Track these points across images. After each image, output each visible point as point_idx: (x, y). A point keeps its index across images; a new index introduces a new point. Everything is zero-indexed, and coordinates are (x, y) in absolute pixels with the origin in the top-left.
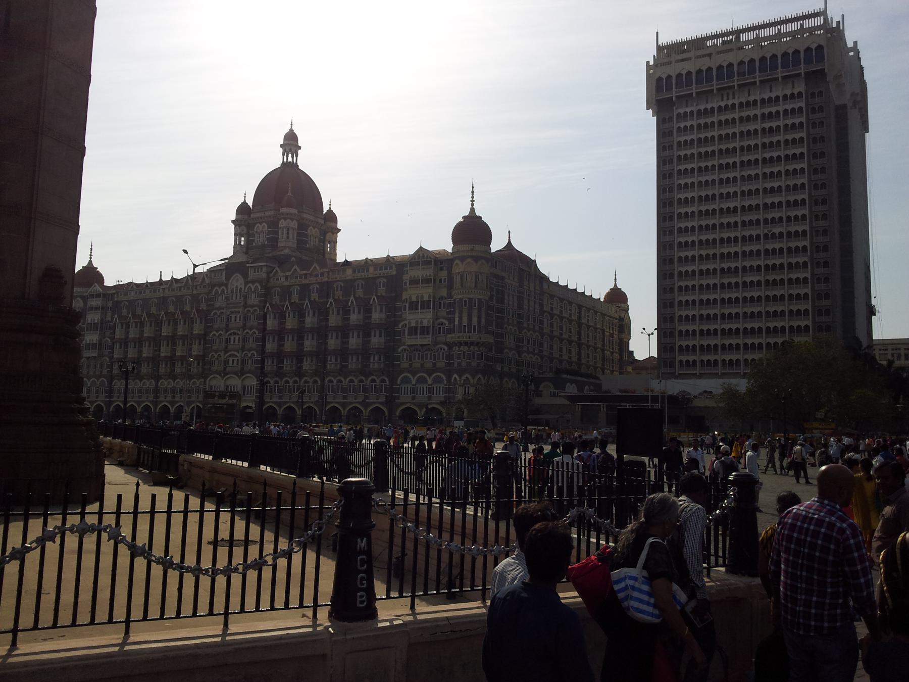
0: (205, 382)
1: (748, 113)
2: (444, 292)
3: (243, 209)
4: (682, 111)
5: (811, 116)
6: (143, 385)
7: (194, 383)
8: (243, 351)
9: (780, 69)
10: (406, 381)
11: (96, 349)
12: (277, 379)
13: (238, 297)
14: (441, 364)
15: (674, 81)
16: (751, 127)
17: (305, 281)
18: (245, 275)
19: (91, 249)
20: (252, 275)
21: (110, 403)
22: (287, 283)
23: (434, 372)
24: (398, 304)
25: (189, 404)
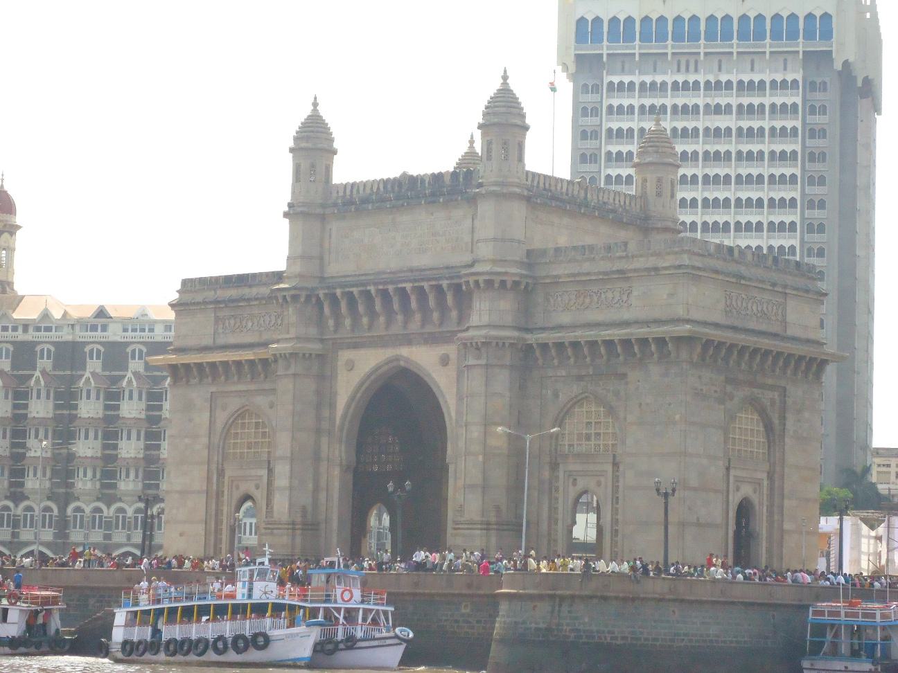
1: (718, 100)
4: (616, 79)
5: (809, 119)
16: (722, 122)
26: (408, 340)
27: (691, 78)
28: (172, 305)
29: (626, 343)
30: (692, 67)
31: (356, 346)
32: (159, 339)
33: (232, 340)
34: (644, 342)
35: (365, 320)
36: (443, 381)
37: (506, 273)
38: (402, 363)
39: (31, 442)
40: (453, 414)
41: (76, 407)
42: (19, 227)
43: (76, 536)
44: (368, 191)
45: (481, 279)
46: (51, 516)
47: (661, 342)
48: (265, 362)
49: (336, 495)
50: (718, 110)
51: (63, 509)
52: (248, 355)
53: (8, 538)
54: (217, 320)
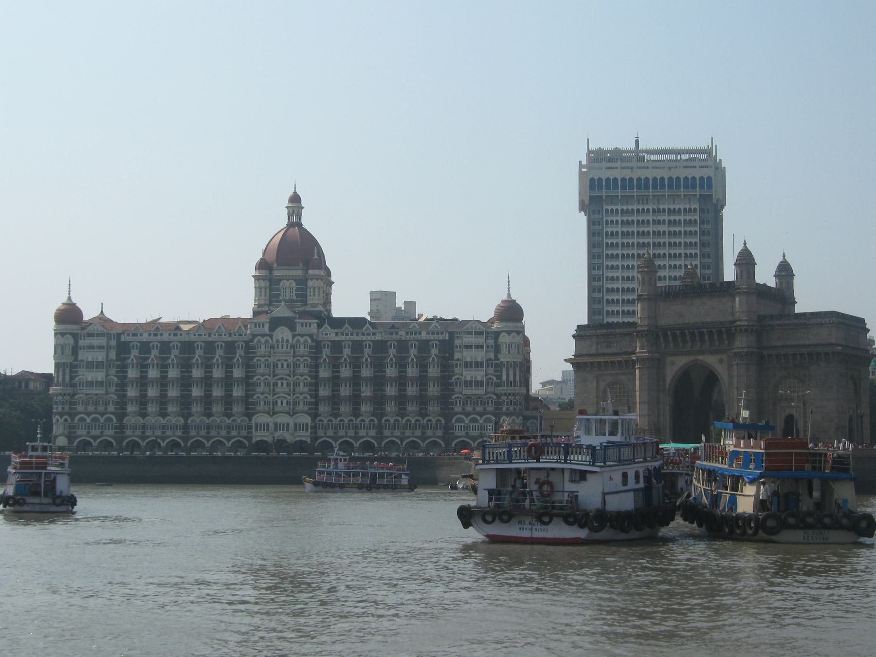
0: (250, 420)
2: (492, 356)
3: (262, 265)
4: (609, 208)
6: (167, 421)
7: (234, 420)
8: (294, 394)
9: (682, 189)
10: (460, 420)
11: (103, 386)
12: (332, 418)
13: (285, 347)
14: (490, 408)
15: (604, 184)
16: (661, 228)
17: (355, 337)
18: (292, 328)
19: (70, 285)
20: (299, 329)
21: (123, 439)
22: (337, 339)
23: (484, 414)
24: (450, 362)
25: (228, 439)
26: (702, 353)
27: (646, 207)
28: (574, 336)
29: (810, 355)
30: (645, 202)
31: (675, 355)
32: (425, 338)
33: (606, 351)
34: (818, 354)
35: (681, 344)
36: (721, 370)
37: (753, 325)
38: (699, 362)
39: (363, 389)
40: (727, 384)
41: (385, 372)
42: (334, 283)
43: (387, 433)
44: (678, 289)
45: (743, 328)
46: (374, 424)
47: (827, 354)
48: (627, 362)
49: (668, 418)
50: (659, 222)
51: (380, 421)
52: (619, 358)
53: (353, 434)
54: (597, 343)
